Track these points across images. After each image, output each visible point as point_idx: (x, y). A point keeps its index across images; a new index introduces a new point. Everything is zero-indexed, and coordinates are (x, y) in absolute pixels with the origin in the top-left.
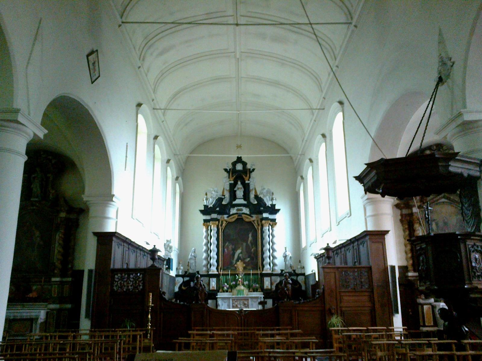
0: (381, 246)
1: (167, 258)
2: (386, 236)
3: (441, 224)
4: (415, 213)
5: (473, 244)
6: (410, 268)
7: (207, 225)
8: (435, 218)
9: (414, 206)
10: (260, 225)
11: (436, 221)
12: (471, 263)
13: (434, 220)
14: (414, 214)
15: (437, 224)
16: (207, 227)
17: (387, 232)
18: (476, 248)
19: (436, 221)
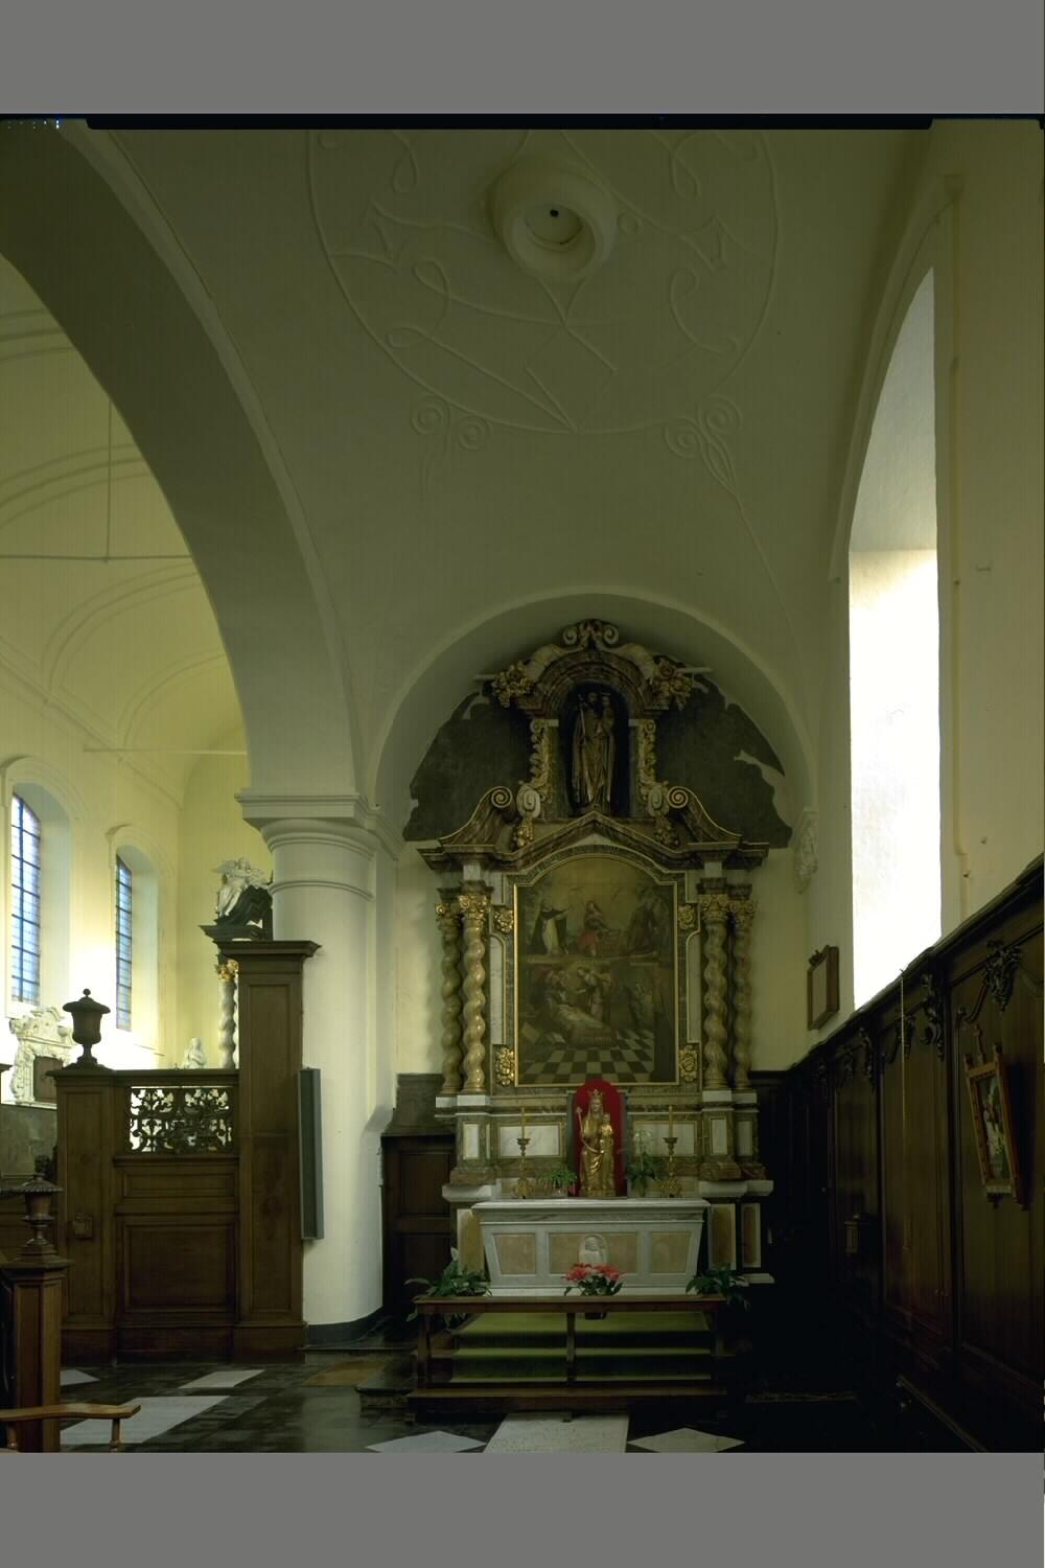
3: (574, 926)
4: (470, 883)
8: (558, 908)
11: (559, 917)
13: (553, 913)
14: (466, 887)
15: (561, 927)
19: (559, 917)
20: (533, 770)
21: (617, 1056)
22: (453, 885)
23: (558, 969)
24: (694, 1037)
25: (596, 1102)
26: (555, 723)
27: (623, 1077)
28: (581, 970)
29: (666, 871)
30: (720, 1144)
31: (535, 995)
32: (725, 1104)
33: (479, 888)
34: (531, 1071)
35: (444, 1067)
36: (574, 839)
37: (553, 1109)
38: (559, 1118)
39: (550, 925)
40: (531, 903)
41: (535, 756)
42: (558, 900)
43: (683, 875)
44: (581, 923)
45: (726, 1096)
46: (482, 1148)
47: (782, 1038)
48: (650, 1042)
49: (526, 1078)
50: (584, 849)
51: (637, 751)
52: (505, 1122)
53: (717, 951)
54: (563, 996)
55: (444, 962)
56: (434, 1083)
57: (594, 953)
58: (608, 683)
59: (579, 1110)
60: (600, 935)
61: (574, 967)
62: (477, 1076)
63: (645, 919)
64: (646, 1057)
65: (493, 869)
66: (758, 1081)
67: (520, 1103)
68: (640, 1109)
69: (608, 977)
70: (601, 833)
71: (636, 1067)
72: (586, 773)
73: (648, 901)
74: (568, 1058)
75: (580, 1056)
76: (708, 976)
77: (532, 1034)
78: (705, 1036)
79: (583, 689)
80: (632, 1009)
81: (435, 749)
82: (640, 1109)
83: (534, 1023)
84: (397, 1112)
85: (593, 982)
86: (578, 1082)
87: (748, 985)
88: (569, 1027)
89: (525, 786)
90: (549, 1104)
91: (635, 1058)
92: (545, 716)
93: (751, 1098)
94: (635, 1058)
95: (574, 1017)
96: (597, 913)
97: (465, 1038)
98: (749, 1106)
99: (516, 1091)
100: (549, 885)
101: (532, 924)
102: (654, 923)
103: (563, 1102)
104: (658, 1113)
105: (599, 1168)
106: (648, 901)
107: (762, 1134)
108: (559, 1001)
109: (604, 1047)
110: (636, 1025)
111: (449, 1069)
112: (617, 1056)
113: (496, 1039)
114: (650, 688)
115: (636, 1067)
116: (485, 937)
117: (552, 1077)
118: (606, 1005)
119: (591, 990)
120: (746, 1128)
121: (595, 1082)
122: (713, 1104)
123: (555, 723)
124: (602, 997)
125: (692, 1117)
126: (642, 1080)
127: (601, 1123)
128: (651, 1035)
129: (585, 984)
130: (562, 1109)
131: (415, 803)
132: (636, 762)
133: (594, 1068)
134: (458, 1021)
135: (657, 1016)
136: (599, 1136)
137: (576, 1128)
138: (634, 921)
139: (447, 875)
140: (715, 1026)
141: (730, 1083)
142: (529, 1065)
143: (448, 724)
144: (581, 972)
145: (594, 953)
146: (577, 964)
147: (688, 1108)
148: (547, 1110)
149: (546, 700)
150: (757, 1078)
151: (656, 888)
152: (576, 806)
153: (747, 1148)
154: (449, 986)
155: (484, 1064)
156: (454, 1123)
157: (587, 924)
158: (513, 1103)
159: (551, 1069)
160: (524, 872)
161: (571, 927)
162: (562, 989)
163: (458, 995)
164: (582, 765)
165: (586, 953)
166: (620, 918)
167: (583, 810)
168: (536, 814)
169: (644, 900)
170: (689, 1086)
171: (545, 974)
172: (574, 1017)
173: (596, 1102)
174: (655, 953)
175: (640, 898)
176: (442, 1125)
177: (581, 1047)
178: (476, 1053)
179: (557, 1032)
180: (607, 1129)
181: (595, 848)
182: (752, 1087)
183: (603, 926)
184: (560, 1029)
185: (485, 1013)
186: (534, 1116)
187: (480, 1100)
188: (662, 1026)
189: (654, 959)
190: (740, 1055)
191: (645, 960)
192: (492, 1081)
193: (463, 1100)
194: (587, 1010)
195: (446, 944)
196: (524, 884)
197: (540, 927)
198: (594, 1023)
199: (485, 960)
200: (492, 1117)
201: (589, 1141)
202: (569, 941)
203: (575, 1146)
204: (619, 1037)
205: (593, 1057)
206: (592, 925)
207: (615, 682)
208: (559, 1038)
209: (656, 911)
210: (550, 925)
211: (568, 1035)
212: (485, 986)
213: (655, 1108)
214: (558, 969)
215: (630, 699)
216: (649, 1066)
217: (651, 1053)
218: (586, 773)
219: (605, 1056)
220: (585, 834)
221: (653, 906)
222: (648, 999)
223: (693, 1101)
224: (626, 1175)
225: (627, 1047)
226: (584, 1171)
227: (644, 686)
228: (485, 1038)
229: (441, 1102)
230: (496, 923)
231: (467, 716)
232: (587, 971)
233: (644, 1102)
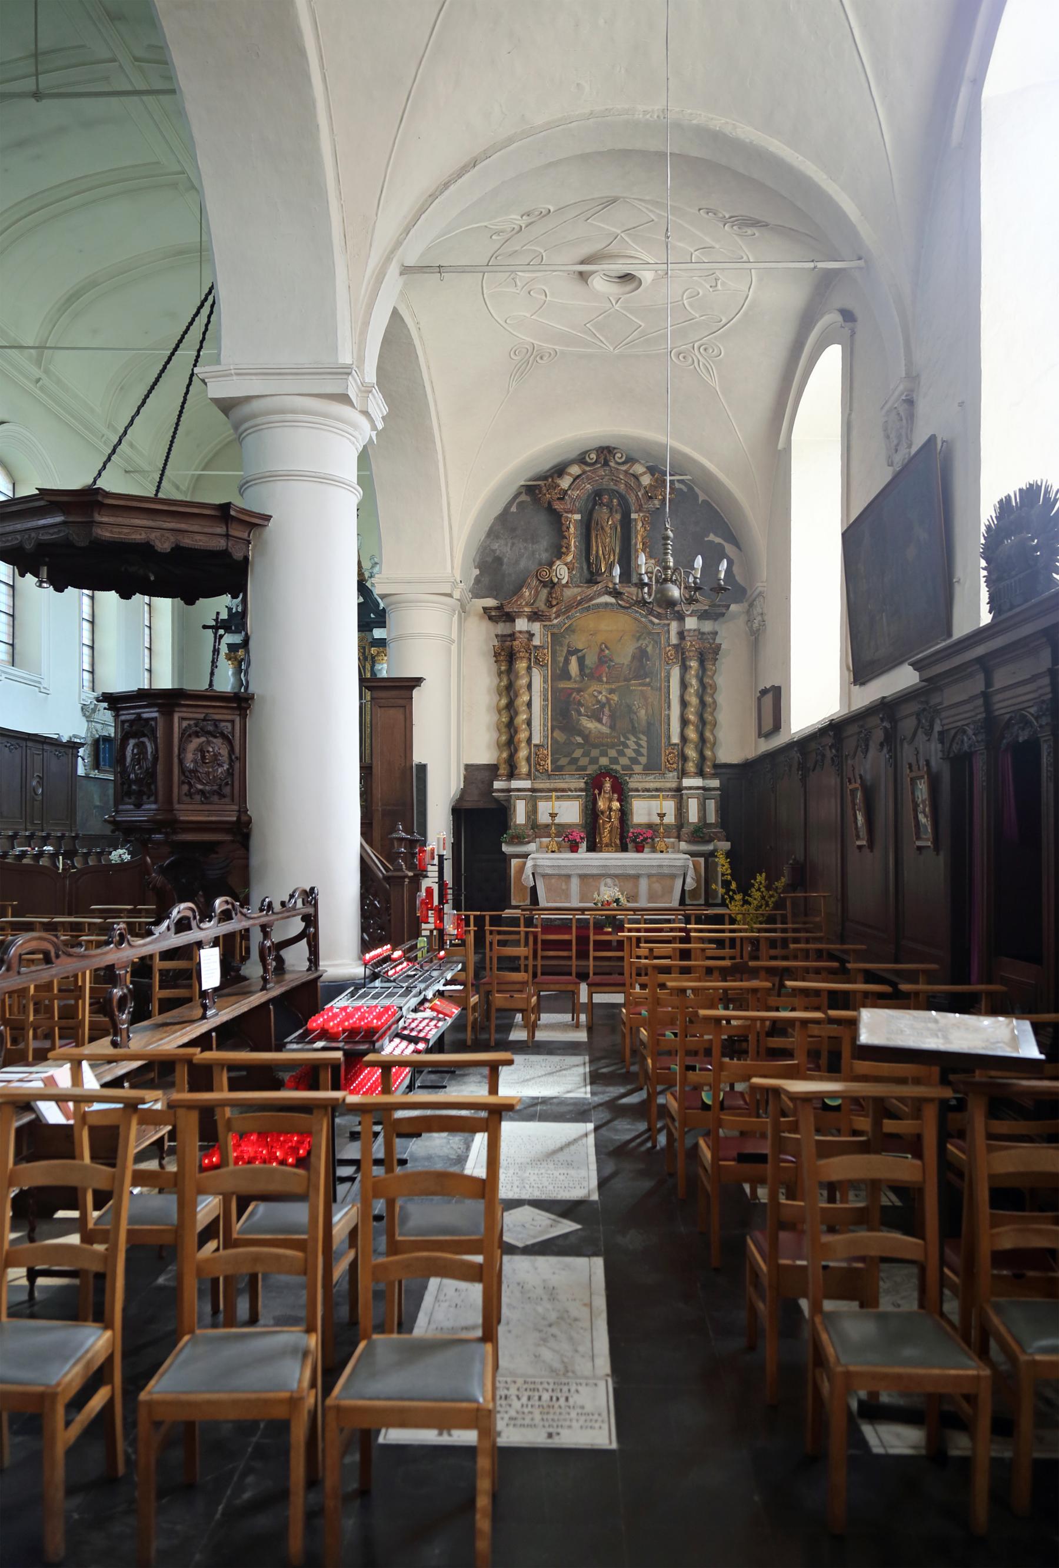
0: (402, 717)
1: (89, 741)
2: (415, 693)
3: (591, 660)
4: (520, 632)
5: (202, 716)
6: (503, 770)
7: (236, 659)
8: (580, 647)
9: (519, 614)
10: (369, 658)
11: (580, 654)
12: (181, 762)
13: (577, 651)
14: (518, 635)
15: (581, 661)
16: (236, 663)
17: (417, 681)
18: (211, 728)
20: (564, 550)
21: (621, 753)
22: (509, 632)
23: (579, 691)
24: (675, 739)
25: (608, 786)
26: (578, 517)
27: (624, 768)
28: (599, 691)
29: (656, 621)
30: (693, 816)
31: (563, 712)
32: (698, 788)
33: (527, 636)
34: (560, 763)
35: (498, 759)
36: (591, 599)
37: (576, 791)
38: (579, 797)
39: (574, 660)
40: (562, 645)
41: (565, 541)
42: (579, 641)
43: (669, 625)
44: (595, 659)
45: (698, 782)
46: (528, 817)
47: (734, 744)
48: (644, 743)
49: (558, 768)
50: (598, 605)
51: (636, 537)
52: (541, 798)
53: (694, 682)
54: (582, 710)
55: (498, 686)
56: (492, 770)
57: (605, 679)
58: (615, 488)
59: (597, 792)
60: (609, 667)
61: (590, 690)
62: (524, 769)
63: (641, 655)
64: (640, 754)
65: (534, 621)
66: (719, 771)
67: (552, 786)
68: (637, 790)
69: (615, 697)
70: (609, 594)
71: (634, 761)
72: (601, 552)
73: (643, 643)
74: (586, 754)
75: (595, 753)
76: (687, 698)
77: (560, 736)
78: (684, 739)
79: (598, 494)
80: (632, 721)
81: (492, 533)
82: (637, 790)
83: (562, 729)
84: (464, 792)
85: (604, 700)
86: (591, 770)
87: (715, 702)
88: (587, 732)
89: (558, 563)
90: (573, 786)
91: (634, 755)
92: (571, 512)
93: (715, 783)
94: (634, 755)
95: (590, 725)
96: (607, 652)
97: (516, 740)
98: (714, 789)
99: (549, 776)
100: (573, 631)
101: (562, 659)
102: (648, 659)
103: (582, 785)
104: (654, 793)
105: (610, 832)
106: (643, 643)
107: (723, 809)
108: (580, 714)
109: (613, 746)
110: (634, 731)
111: (502, 761)
112: (621, 753)
113: (536, 740)
114: (647, 492)
115: (634, 761)
116: (529, 668)
117: (574, 767)
118: (612, 717)
119: (603, 706)
120: (711, 805)
121: (607, 773)
122: (690, 788)
123: (578, 517)
124: (610, 710)
125: (673, 797)
126: (638, 768)
127: (611, 800)
128: (645, 738)
129: (598, 702)
130: (581, 790)
131: (477, 572)
132: (636, 544)
133: (604, 761)
134: (511, 727)
135: (649, 724)
136: (610, 809)
137: (595, 802)
138: (634, 657)
139: (501, 625)
140: (692, 734)
141: (701, 773)
142: (559, 759)
143: (500, 515)
144: (596, 693)
145: (605, 679)
146: (594, 687)
147: (670, 790)
148: (571, 791)
149: (573, 501)
150: (720, 769)
151: (650, 633)
152: (592, 577)
153: (712, 818)
154: (504, 702)
155: (528, 759)
156: (508, 800)
157: (600, 659)
158: (547, 786)
159: (574, 761)
160: (555, 622)
161: (588, 662)
162: (582, 706)
163: (511, 707)
164: (597, 547)
165: (600, 680)
166: (624, 655)
167: (599, 579)
168: (564, 582)
169: (640, 642)
170: (671, 775)
171: (571, 694)
172: (590, 725)
173: (608, 786)
174: (648, 680)
175: (638, 640)
176: (496, 800)
177: (595, 746)
178: (523, 753)
179: (579, 735)
180: (616, 805)
181: (607, 604)
182: (714, 776)
183: (612, 661)
184: (580, 733)
185: (529, 723)
186: (563, 794)
187: (526, 784)
188: (654, 729)
189: (648, 685)
190: (708, 753)
191: (641, 685)
192: (533, 770)
193: (515, 784)
194: (600, 721)
195: (500, 674)
196: (556, 631)
197: (567, 661)
198: (605, 730)
199: (529, 686)
200: (533, 796)
201: (602, 813)
202: (587, 671)
203: (592, 814)
204: (622, 739)
205: (604, 754)
206: (603, 660)
207: (622, 487)
208: (579, 740)
209: (649, 649)
210: (574, 660)
211: (586, 738)
212: (529, 704)
213: (648, 790)
214: (579, 691)
215: (632, 499)
216: (643, 760)
217: (644, 751)
218: (601, 552)
219: (613, 753)
220: (600, 595)
221: (647, 646)
222: (643, 712)
223: (674, 785)
224: (629, 838)
225: (627, 747)
226: (600, 834)
227: (643, 491)
228: (529, 740)
229: (497, 785)
230: (536, 658)
231: (514, 509)
232: (600, 693)
233: (640, 786)
